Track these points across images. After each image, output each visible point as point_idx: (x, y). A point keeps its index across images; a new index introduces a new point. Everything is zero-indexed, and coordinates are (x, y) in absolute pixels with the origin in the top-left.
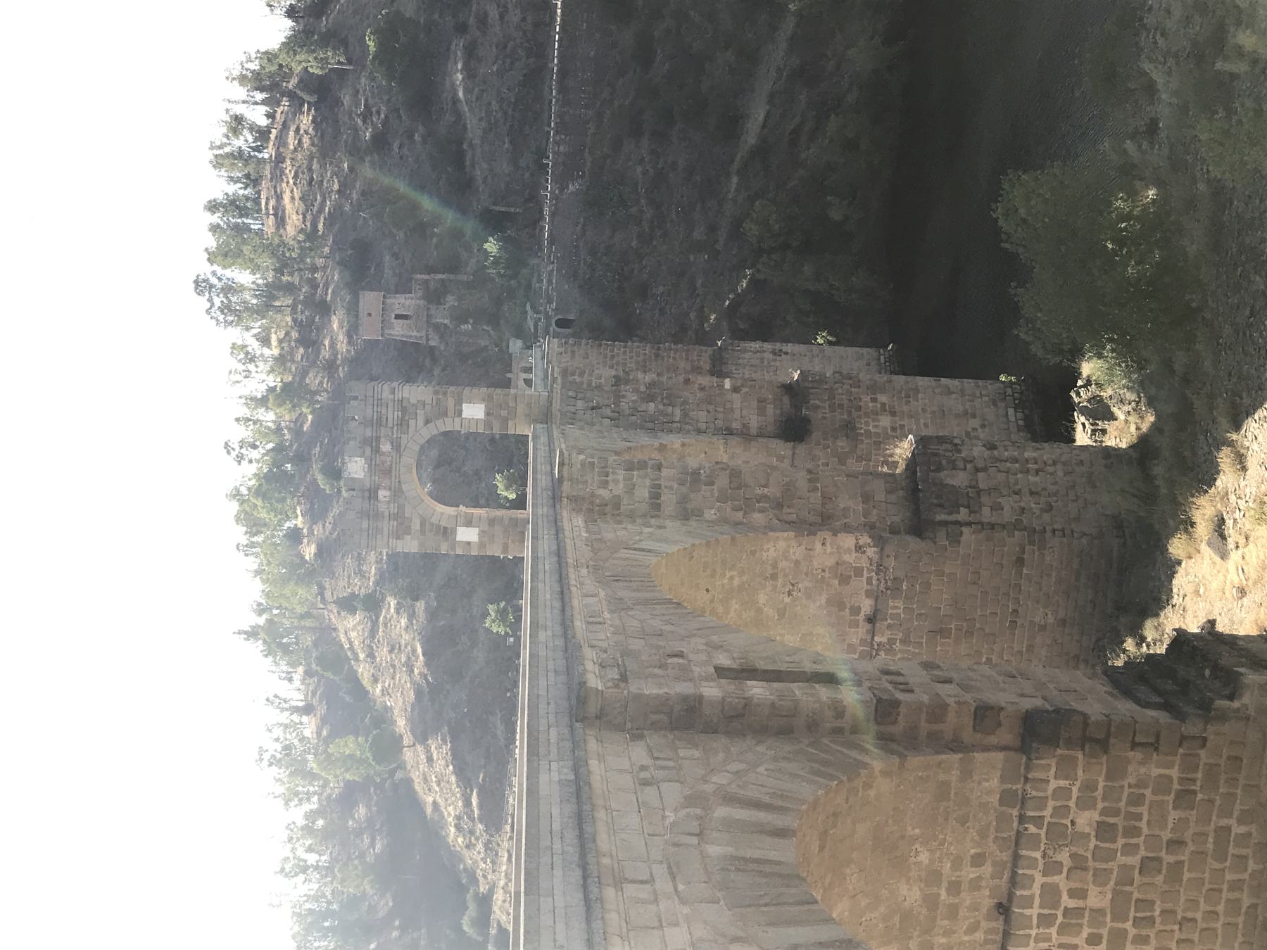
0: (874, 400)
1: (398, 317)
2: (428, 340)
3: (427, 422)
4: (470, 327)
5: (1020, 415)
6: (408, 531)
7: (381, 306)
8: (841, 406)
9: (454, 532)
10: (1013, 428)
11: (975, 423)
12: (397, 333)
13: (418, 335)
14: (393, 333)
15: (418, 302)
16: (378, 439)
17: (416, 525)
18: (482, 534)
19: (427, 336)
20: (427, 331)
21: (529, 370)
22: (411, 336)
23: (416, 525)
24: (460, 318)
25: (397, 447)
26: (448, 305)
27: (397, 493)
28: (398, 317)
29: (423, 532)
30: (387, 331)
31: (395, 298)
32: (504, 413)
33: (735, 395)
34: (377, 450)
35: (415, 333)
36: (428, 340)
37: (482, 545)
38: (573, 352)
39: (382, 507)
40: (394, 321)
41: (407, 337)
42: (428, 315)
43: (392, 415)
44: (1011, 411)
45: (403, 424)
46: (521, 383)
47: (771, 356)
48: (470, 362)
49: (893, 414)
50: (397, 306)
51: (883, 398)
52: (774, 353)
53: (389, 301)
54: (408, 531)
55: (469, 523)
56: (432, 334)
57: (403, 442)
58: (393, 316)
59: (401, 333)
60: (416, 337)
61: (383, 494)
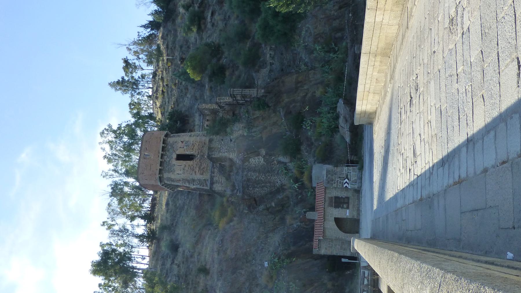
1: (180, 157)
2: (212, 183)
4: (262, 160)
7: (162, 145)
12: (177, 177)
14: (173, 176)
19: (212, 178)
20: (213, 172)
22: (193, 180)
28: (180, 157)
30: (166, 175)
31: (179, 136)
35: (198, 176)
36: (212, 183)
40: (174, 162)
41: (189, 181)
42: (210, 149)
48: (261, 207)
50: (180, 144)
53: (170, 140)
56: (218, 177)
58: (175, 156)
59: (182, 176)
60: (200, 182)
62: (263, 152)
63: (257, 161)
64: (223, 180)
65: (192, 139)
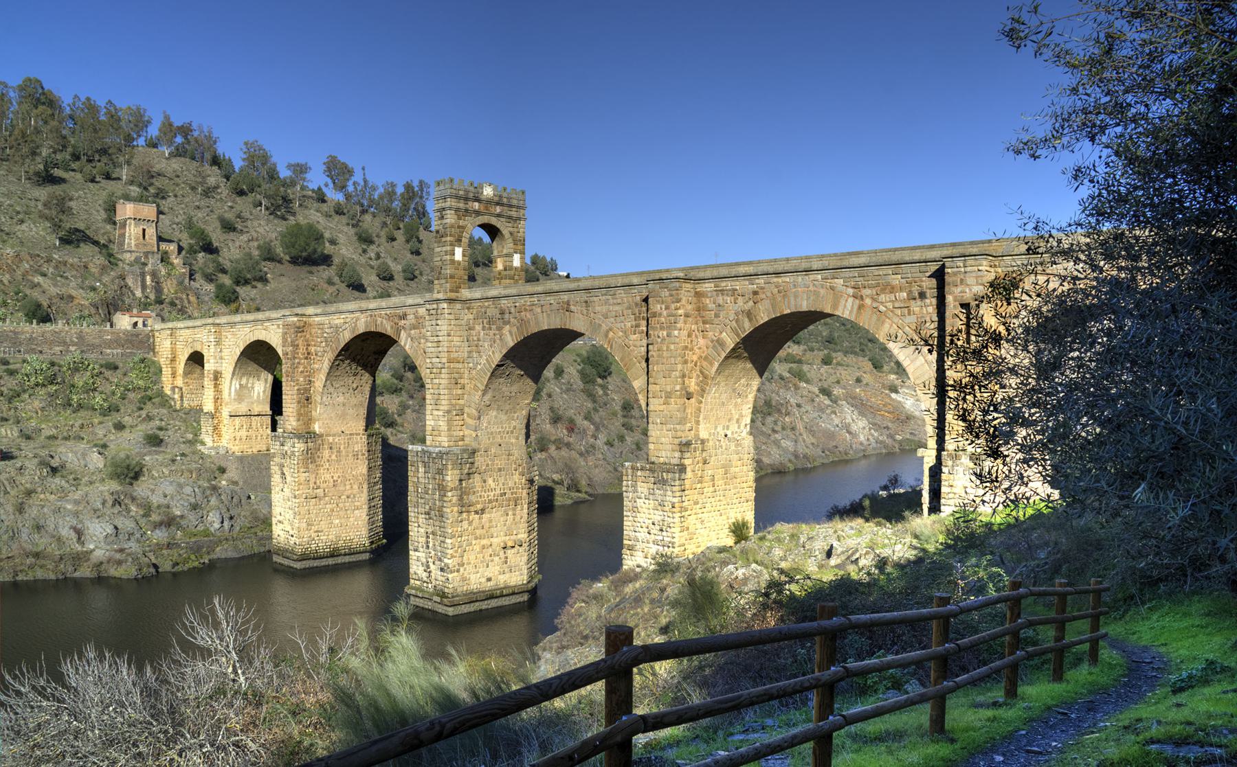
1: (144, 230)
3: (511, 234)
6: (459, 219)
9: (460, 246)
13: (133, 245)
16: (502, 205)
17: (461, 223)
18: (459, 263)
24: (154, 274)
25: (499, 216)
27: (478, 213)
28: (144, 230)
29: (459, 227)
32: (516, 277)
34: (498, 204)
37: (453, 262)
39: (470, 203)
46: (135, 319)
54: (459, 219)
55: (464, 255)
57: (502, 219)
61: (476, 206)
64: (133, 258)
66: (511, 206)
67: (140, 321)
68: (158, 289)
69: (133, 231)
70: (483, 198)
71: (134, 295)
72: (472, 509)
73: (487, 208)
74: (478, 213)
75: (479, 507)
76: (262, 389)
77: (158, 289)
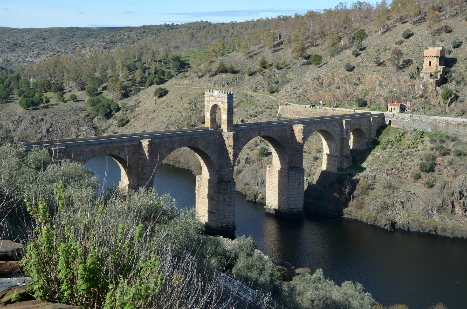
0: (227, 198)
1: (430, 62)
2: (421, 73)
5: (225, 226)
6: (208, 103)
8: (225, 191)
10: (222, 224)
11: (223, 217)
15: (435, 69)
17: (209, 104)
21: (394, 109)
23: (209, 104)
25: (219, 101)
26: (430, 80)
27: (213, 101)
28: (430, 62)
29: (208, 106)
31: (437, 60)
33: (228, 170)
38: (299, 132)
43: (223, 100)
44: (226, 224)
45: (222, 103)
47: (298, 182)
48: (411, 88)
49: (224, 201)
51: (227, 199)
52: (299, 183)
53: (436, 58)
54: (208, 103)
61: (212, 98)
62: (423, 88)
63: (421, 87)
65: (435, 65)
66: (222, 98)
67: (393, 107)
68: (425, 91)
69: (426, 62)
70: (214, 95)
71: (414, 92)
72: (201, 196)
73: (216, 99)
74: (213, 101)
75: (202, 196)
76: (334, 146)
77: (425, 91)
